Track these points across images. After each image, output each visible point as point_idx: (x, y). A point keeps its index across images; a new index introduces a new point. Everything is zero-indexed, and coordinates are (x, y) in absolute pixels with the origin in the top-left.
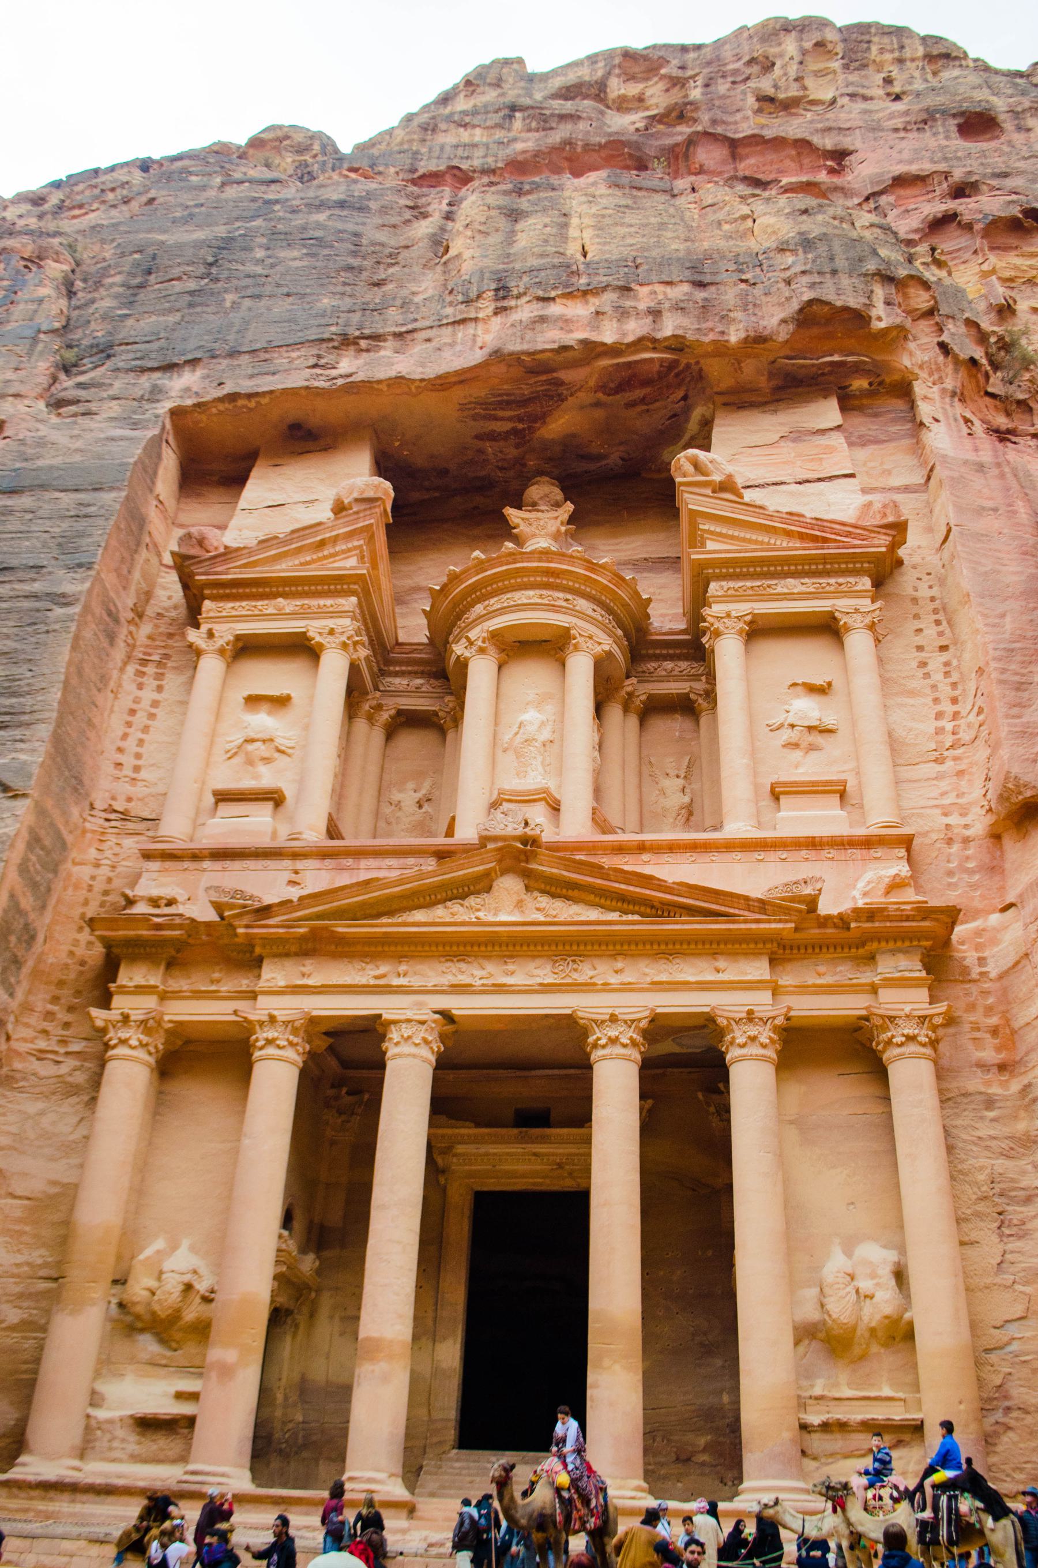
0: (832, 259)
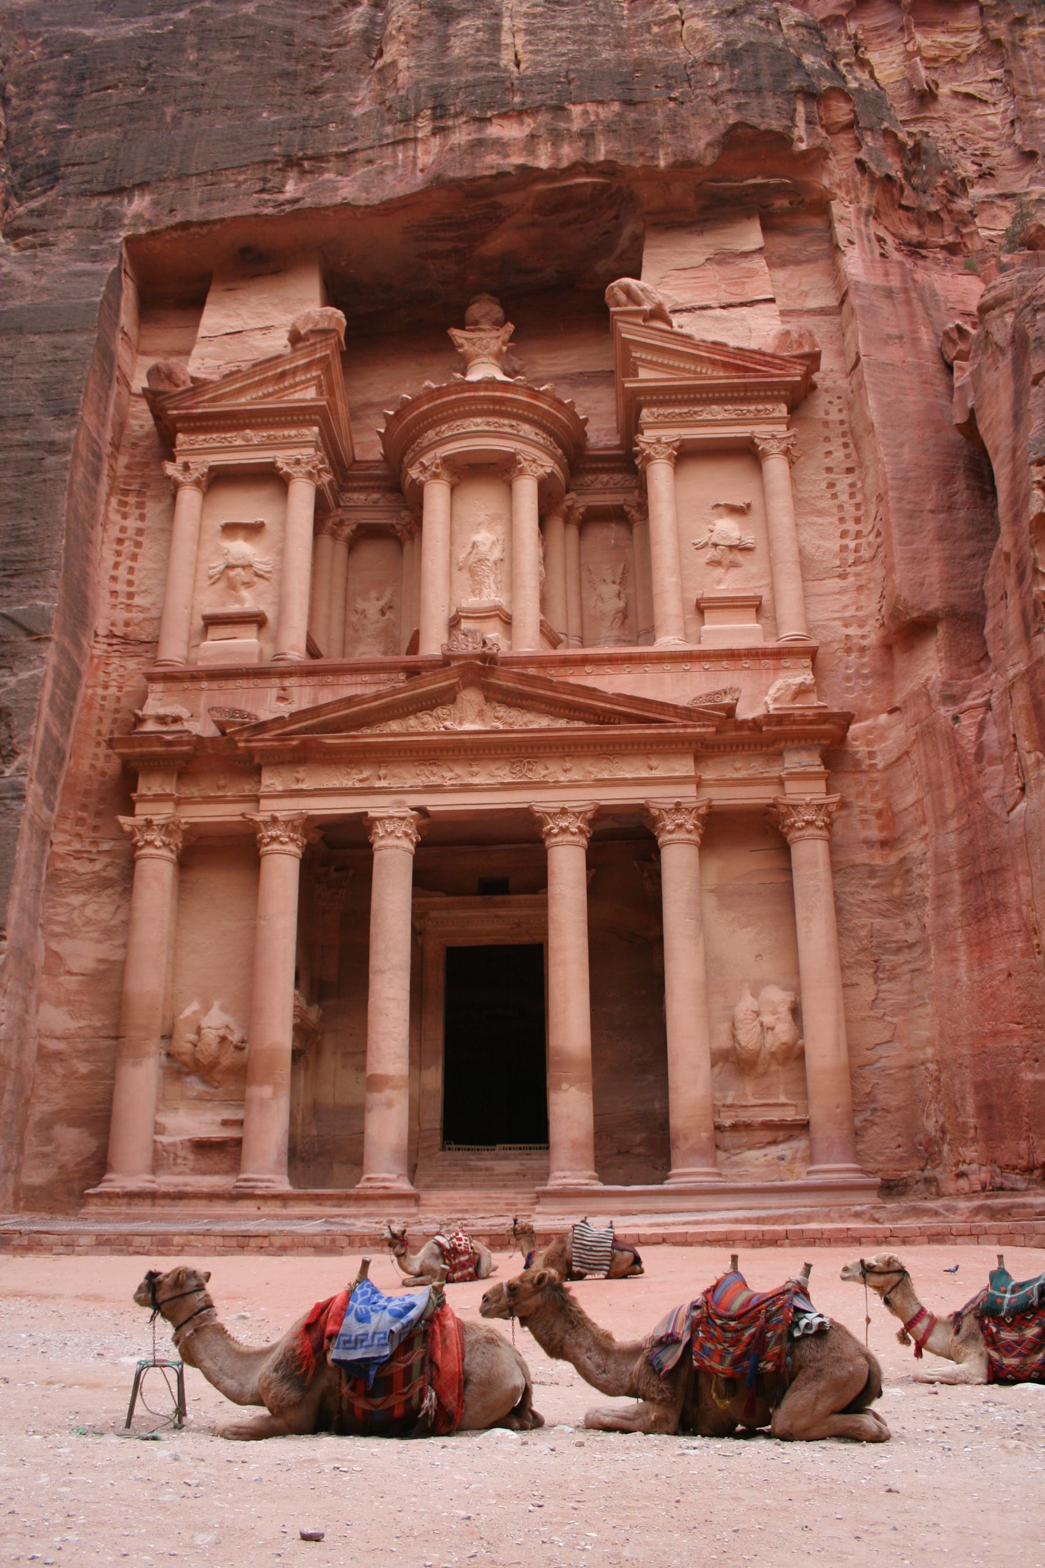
0: (757, 75)
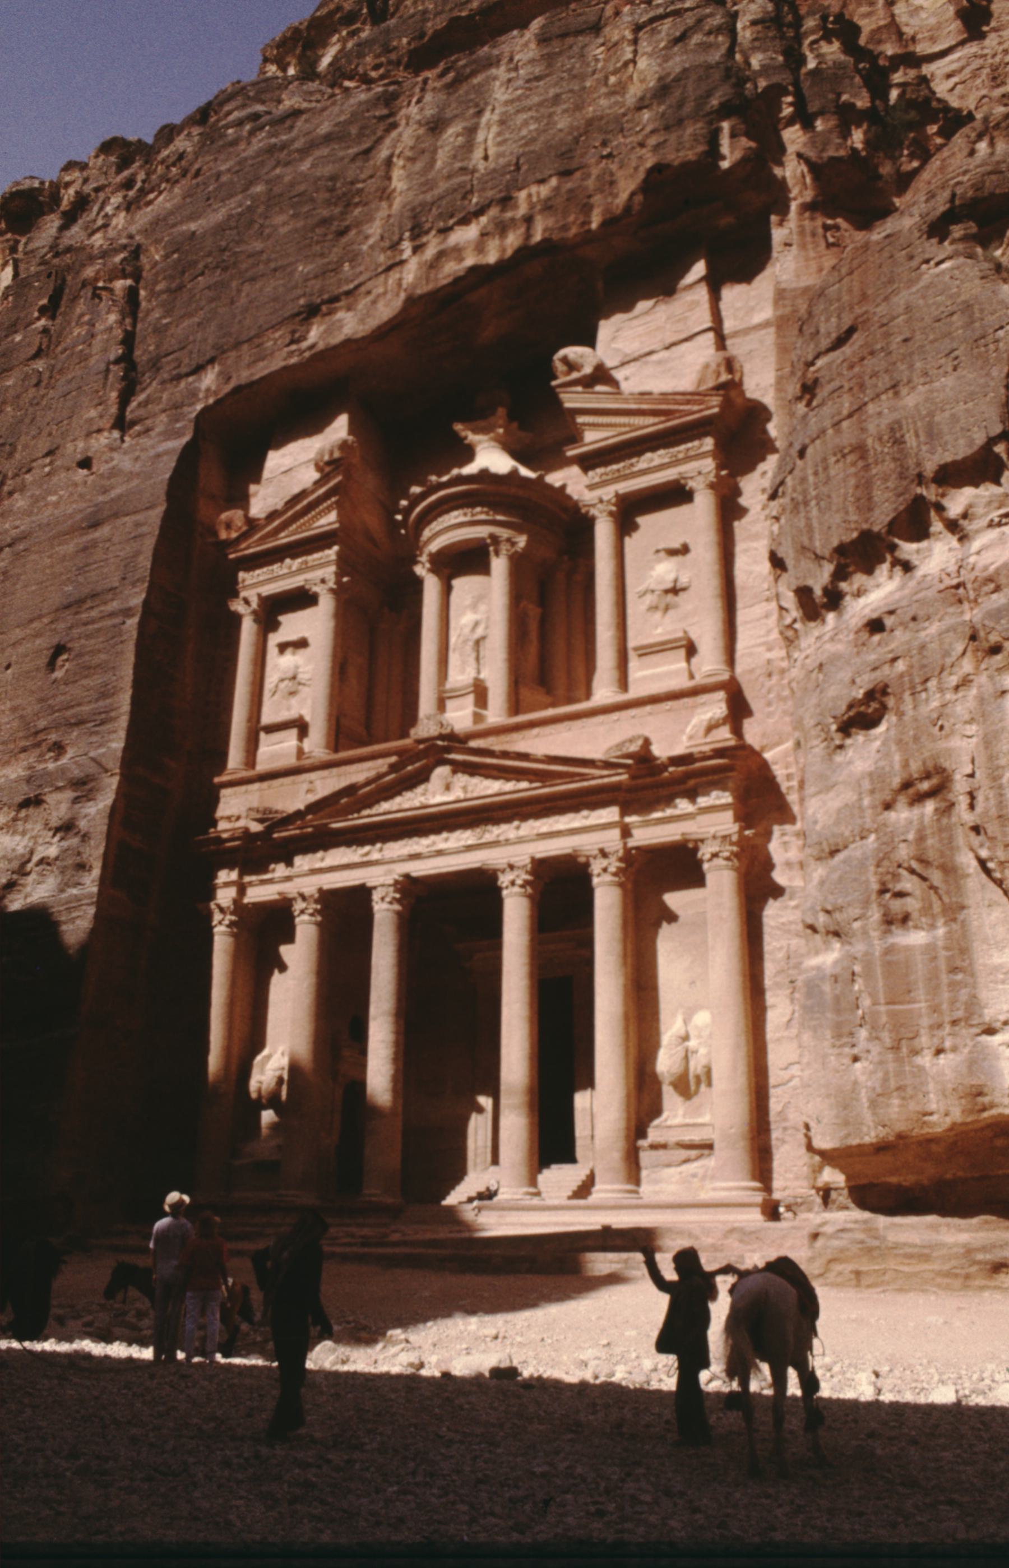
0: (680, 105)
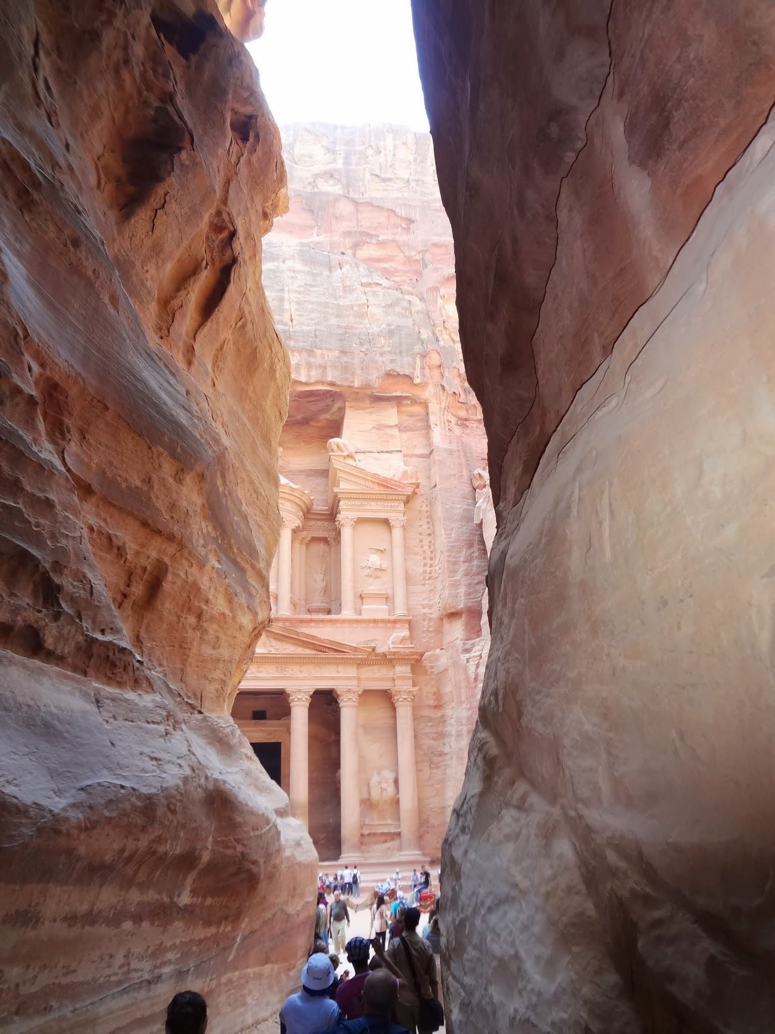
0: (400, 345)
